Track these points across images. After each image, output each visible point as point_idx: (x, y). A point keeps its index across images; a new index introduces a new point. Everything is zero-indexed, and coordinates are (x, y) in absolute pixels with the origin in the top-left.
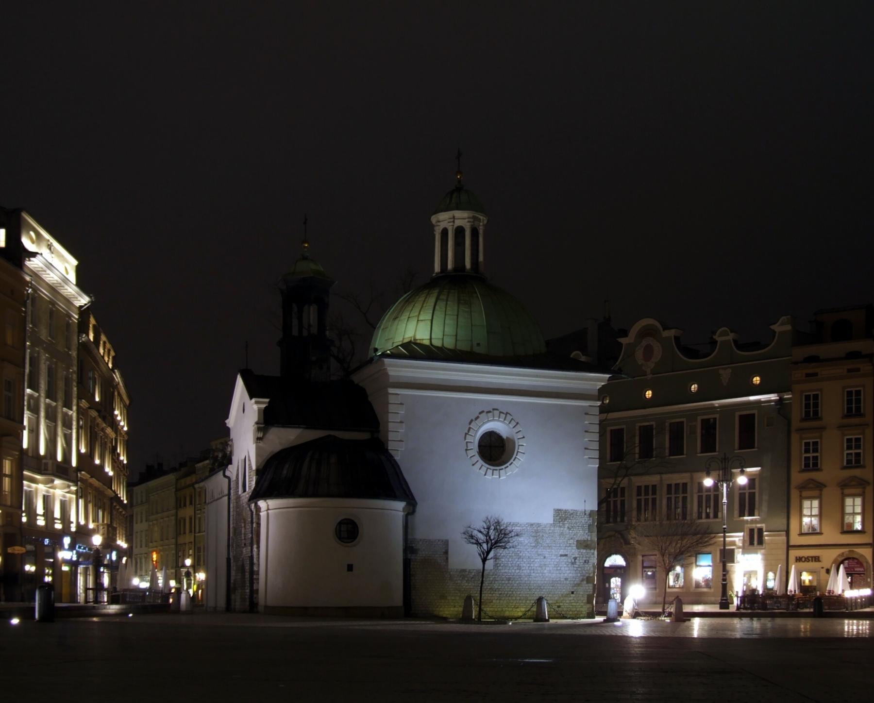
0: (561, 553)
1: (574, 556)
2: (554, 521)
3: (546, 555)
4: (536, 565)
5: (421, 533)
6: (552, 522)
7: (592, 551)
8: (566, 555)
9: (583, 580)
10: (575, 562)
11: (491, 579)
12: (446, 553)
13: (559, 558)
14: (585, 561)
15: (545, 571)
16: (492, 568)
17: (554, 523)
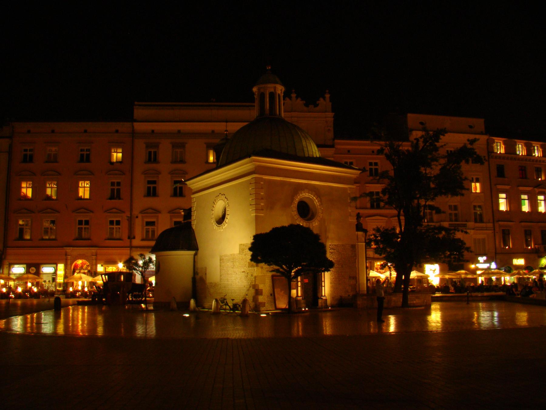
0: (242, 271)
1: (247, 272)
2: (239, 252)
3: (237, 272)
4: (233, 279)
5: (199, 265)
6: (238, 252)
7: (254, 268)
8: (244, 272)
9: (250, 287)
10: (248, 276)
11: (219, 287)
12: (206, 274)
13: (242, 273)
14: (252, 275)
15: (237, 282)
16: (219, 281)
17: (239, 253)
